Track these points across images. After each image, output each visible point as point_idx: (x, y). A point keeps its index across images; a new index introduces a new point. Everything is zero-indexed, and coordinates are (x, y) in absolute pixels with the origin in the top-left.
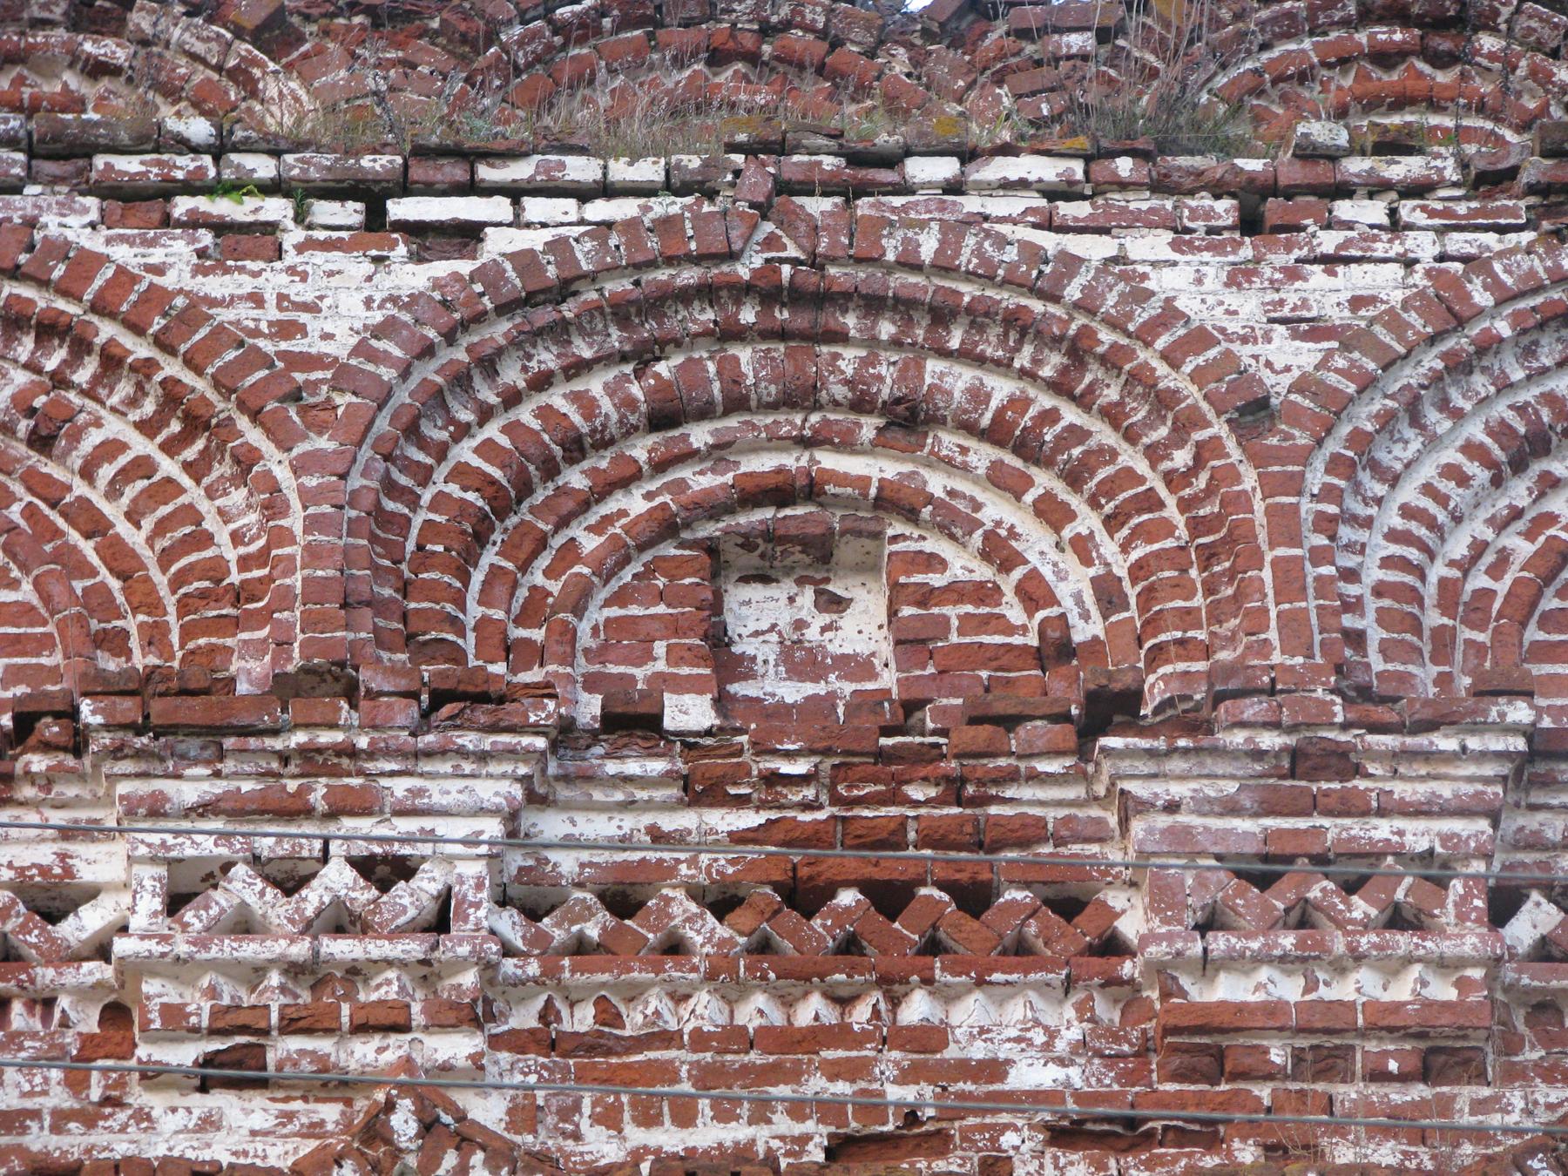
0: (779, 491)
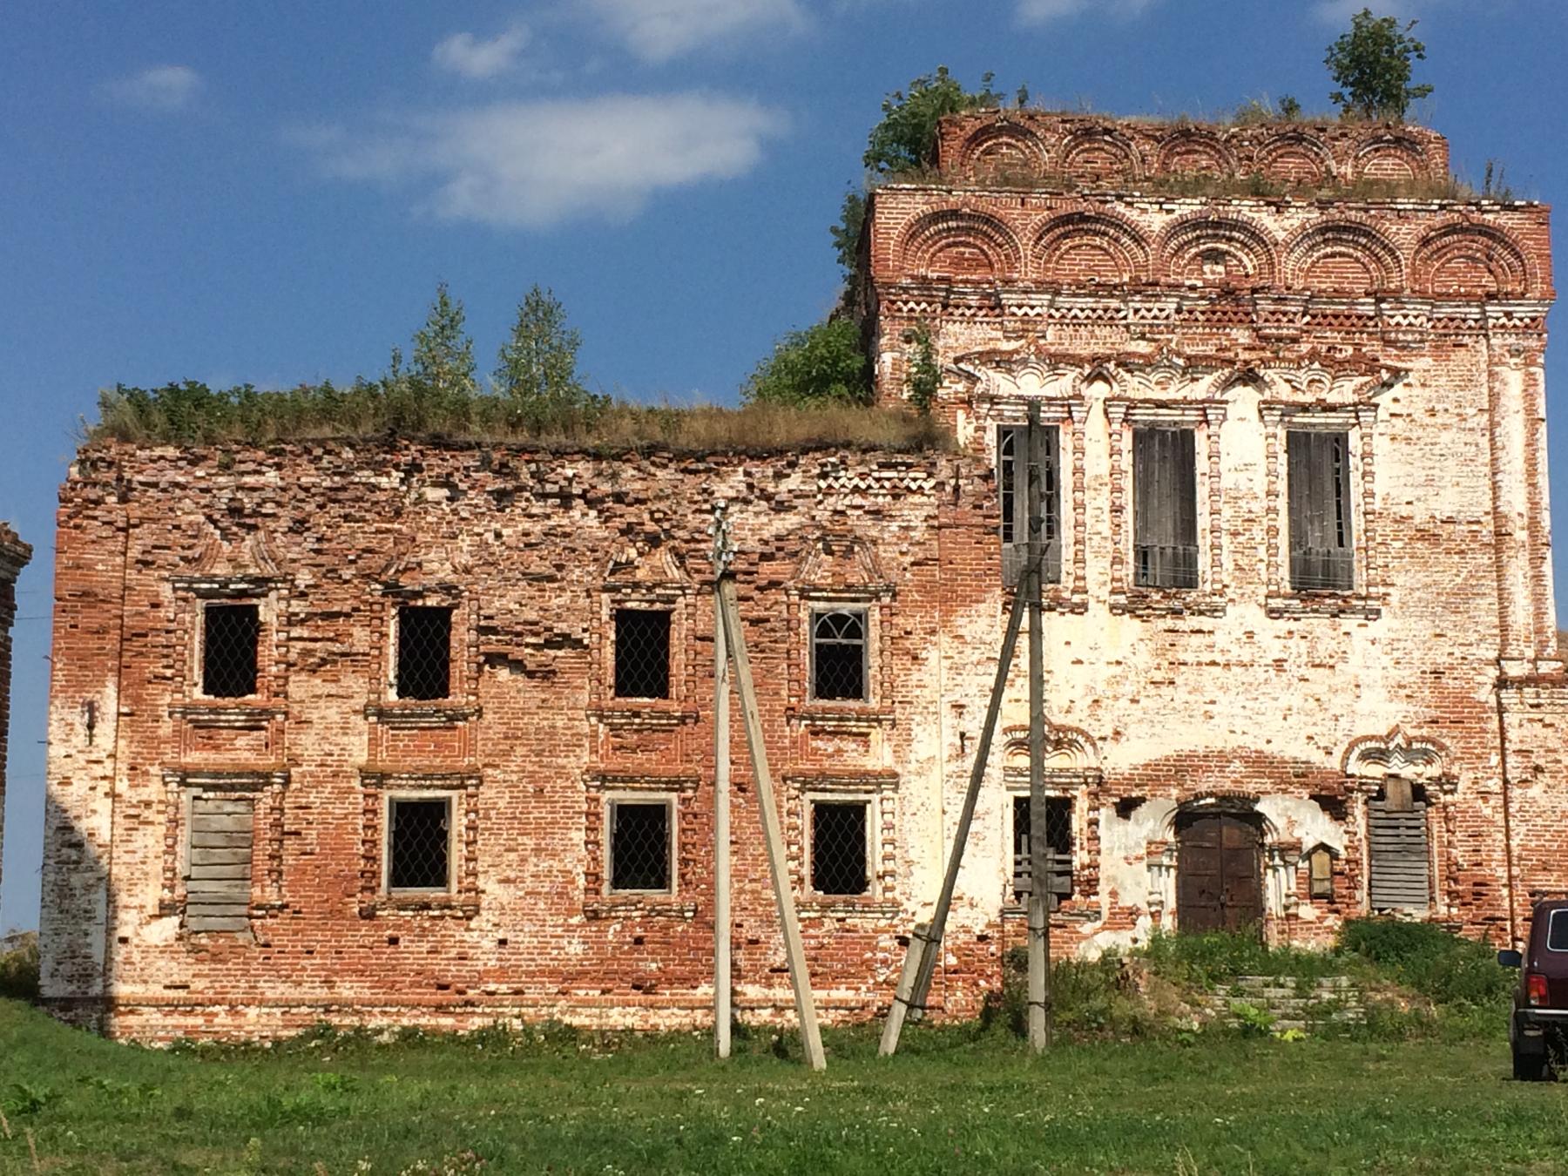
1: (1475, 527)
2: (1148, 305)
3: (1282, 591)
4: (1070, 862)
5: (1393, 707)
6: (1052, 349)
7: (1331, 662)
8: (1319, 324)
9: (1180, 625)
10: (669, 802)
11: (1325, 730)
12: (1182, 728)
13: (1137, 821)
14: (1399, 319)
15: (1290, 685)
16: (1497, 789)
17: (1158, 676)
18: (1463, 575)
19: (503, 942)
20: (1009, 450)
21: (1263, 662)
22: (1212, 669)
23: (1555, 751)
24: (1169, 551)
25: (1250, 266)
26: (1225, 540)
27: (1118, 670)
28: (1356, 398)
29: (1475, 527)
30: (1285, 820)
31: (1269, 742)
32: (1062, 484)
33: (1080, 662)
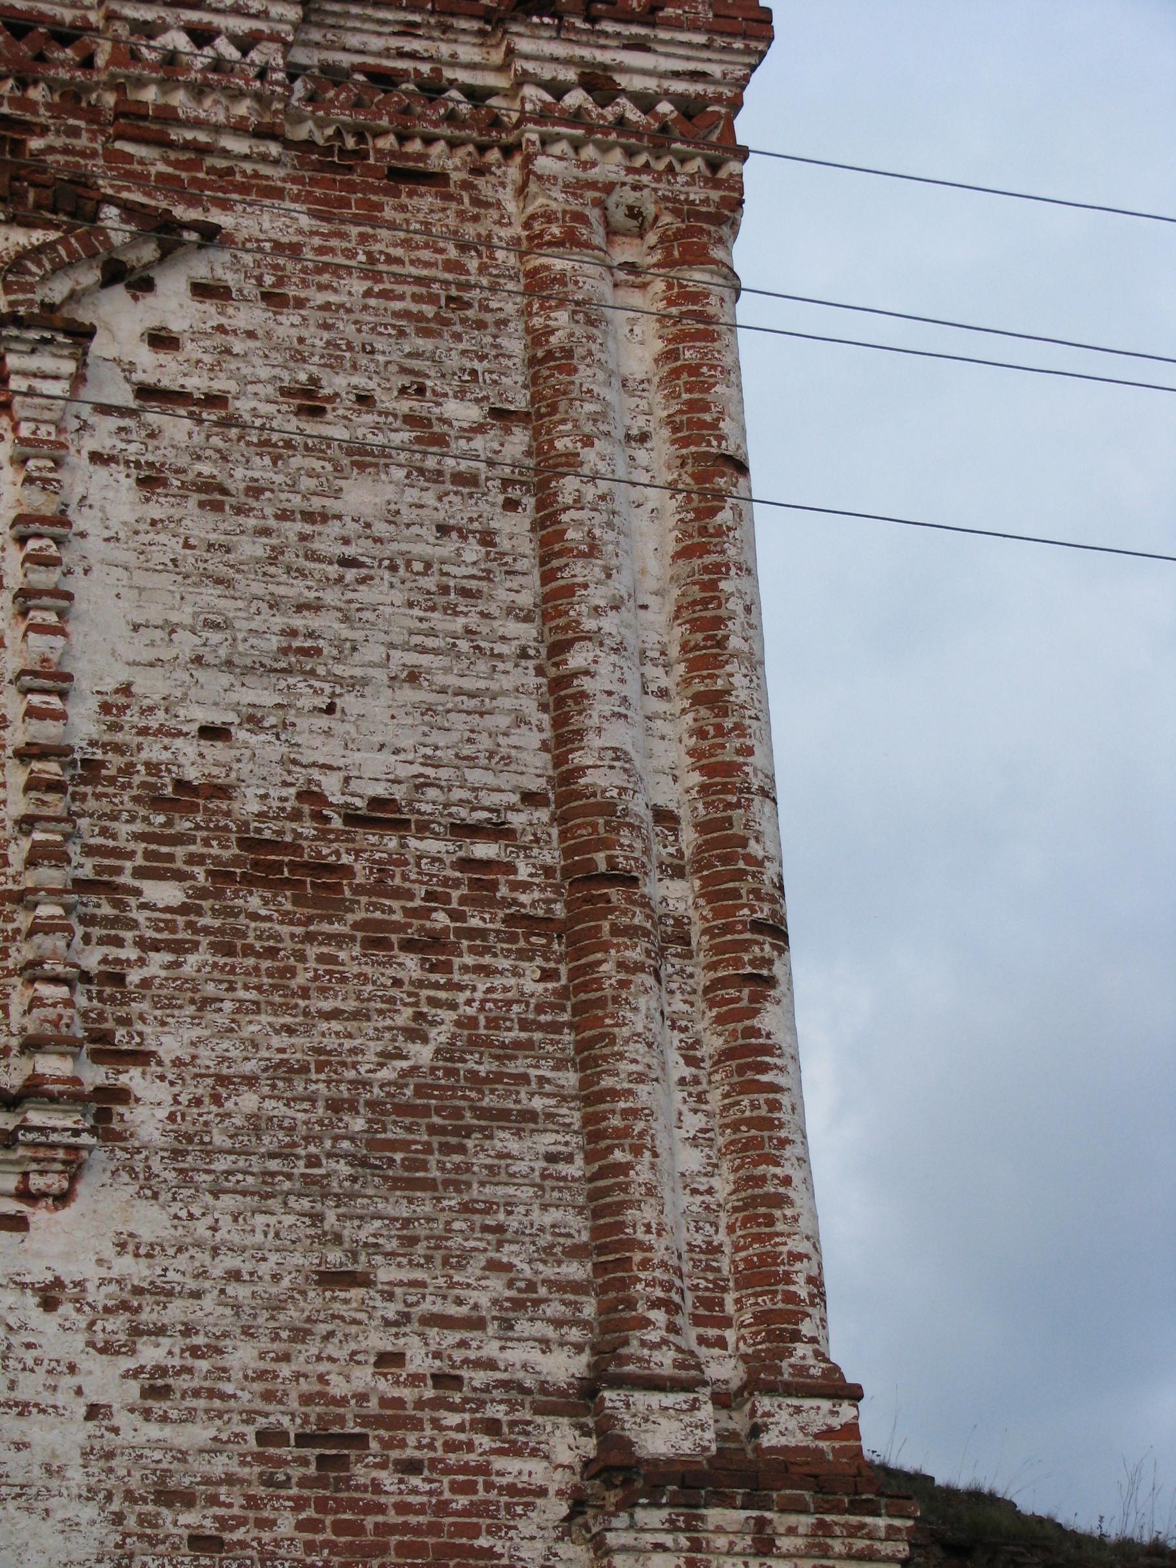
1: (484, 850)
14: (179, 40)
18: (440, 1036)
29: (484, 850)
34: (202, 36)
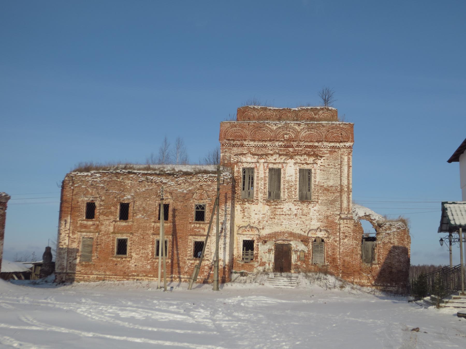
0: (286, 133)
2: (272, 144)
3: (297, 200)
4: (253, 253)
5: (318, 223)
6: (254, 153)
7: (306, 214)
8: (307, 147)
9: (277, 207)
10: (167, 240)
11: (304, 228)
12: (276, 227)
13: (266, 245)
15: (298, 219)
16: (338, 240)
17: (272, 217)
18: (334, 197)
19: (136, 265)
20: (244, 173)
21: (293, 214)
22: (282, 215)
23: (350, 233)
24: (275, 192)
25: (293, 136)
26: (286, 190)
27: (264, 216)
28: (313, 162)
30: (295, 245)
31: (293, 230)
32: (255, 179)
33: (256, 214)
34: (324, 146)
